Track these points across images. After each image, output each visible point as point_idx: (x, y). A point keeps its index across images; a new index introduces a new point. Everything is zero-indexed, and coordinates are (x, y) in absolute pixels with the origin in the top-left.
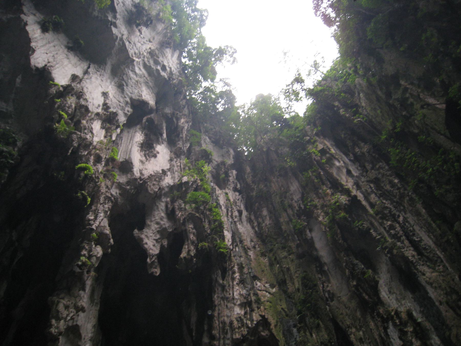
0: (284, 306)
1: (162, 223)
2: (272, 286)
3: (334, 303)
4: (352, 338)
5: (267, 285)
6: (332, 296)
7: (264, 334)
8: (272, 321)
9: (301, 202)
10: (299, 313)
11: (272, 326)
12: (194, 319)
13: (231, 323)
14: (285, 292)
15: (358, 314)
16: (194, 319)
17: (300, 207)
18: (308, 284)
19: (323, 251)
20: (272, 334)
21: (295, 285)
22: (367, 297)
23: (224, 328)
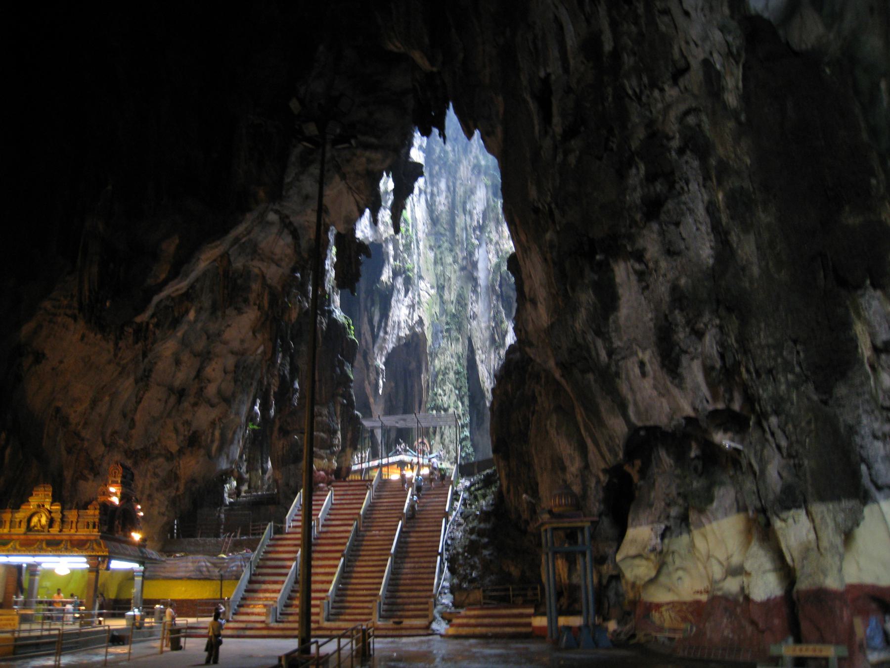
0: (437, 310)
1: (366, 231)
2: (432, 287)
3: (474, 323)
4: (477, 358)
5: (429, 286)
6: (475, 316)
7: (418, 330)
8: (427, 323)
9: (481, 216)
10: (447, 324)
11: (425, 328)
12: (376, 318)
13: (399, 323)
14: (441, 297)
15: (488, 343)
16: (376, 318)
17: (478, 222)
18: (461, 301)
19: (482, 275)
20: (423, 333)
21: (451, 296)
22: (497, 338)
23: (394, 327)
